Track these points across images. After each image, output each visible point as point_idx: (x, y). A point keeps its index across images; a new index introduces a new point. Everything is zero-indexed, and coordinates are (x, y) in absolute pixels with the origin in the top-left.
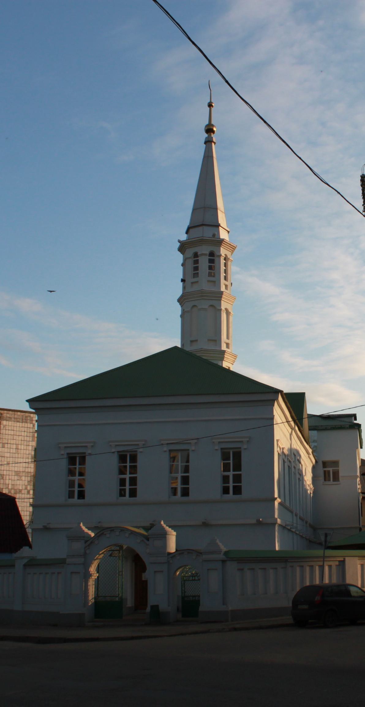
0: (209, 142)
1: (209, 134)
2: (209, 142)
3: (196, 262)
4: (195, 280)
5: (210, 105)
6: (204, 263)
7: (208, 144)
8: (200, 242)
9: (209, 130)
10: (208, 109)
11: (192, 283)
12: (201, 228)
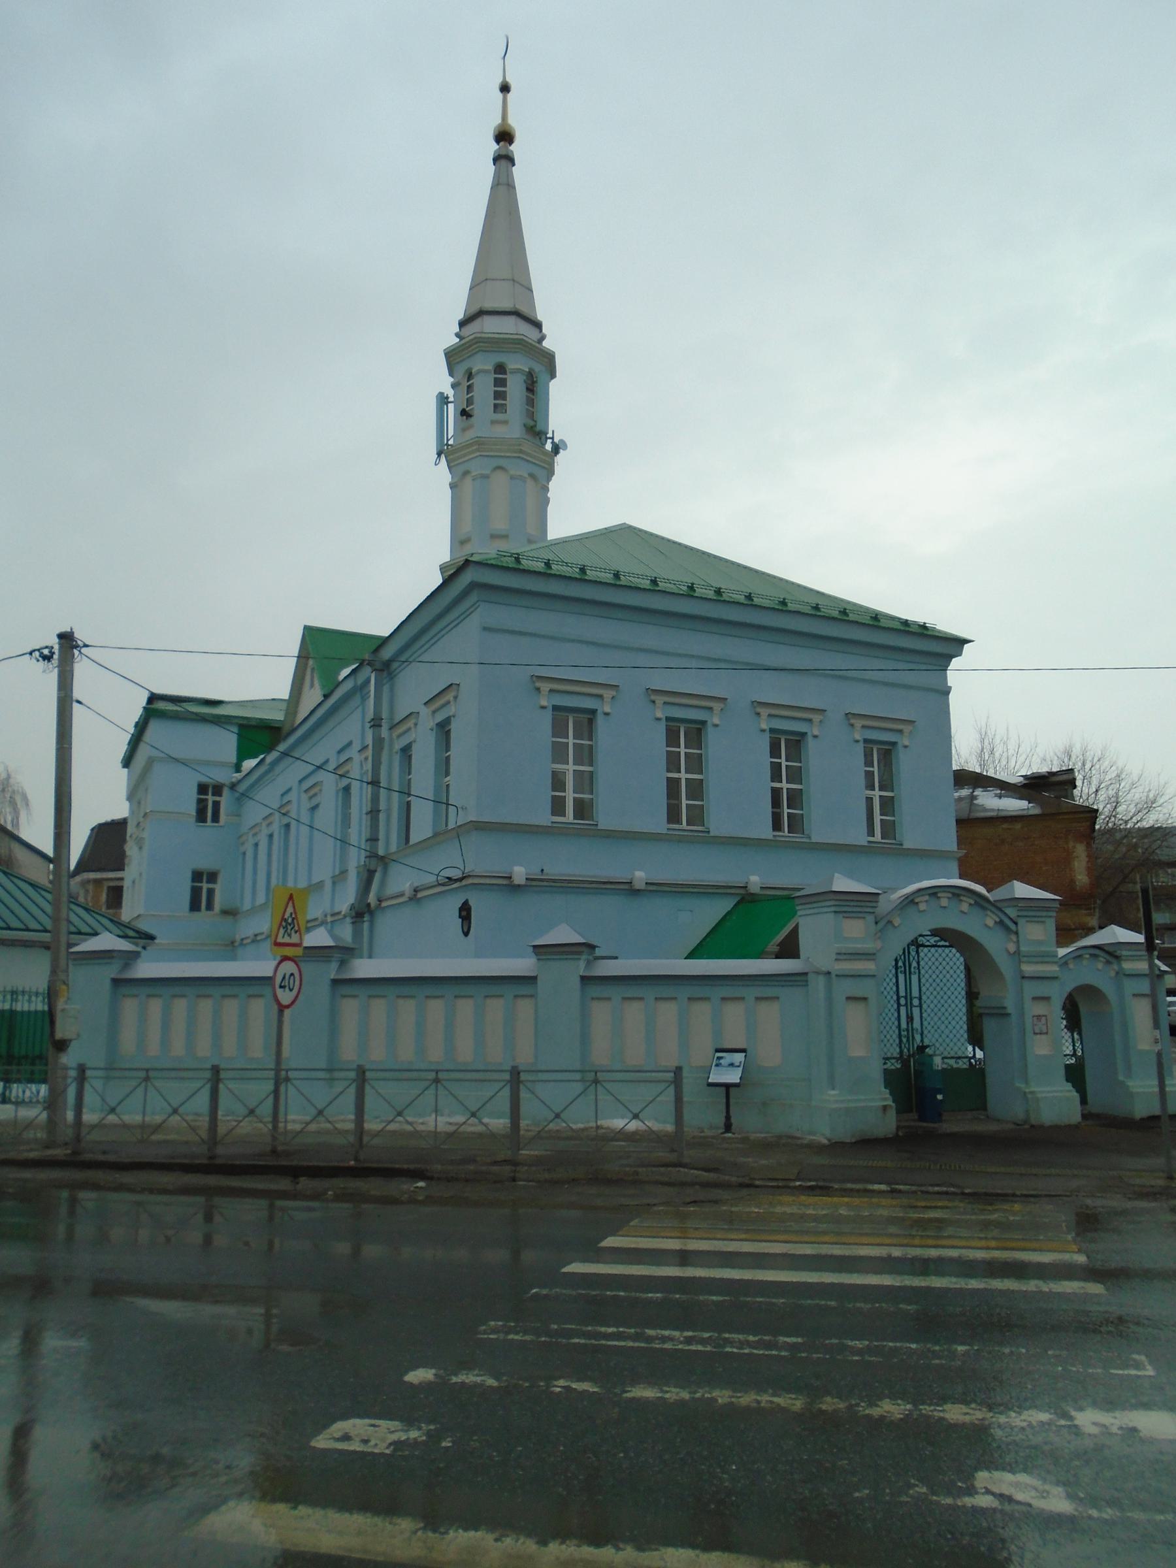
0: (504, 160)
1: (502, 143)
2: (504, 160)
4: (500, 416)
5: (505, 88)
6: (515, 388)
7: (503, 163)
9: (504, 136)
10: (500, 95)
11: (493, 422)
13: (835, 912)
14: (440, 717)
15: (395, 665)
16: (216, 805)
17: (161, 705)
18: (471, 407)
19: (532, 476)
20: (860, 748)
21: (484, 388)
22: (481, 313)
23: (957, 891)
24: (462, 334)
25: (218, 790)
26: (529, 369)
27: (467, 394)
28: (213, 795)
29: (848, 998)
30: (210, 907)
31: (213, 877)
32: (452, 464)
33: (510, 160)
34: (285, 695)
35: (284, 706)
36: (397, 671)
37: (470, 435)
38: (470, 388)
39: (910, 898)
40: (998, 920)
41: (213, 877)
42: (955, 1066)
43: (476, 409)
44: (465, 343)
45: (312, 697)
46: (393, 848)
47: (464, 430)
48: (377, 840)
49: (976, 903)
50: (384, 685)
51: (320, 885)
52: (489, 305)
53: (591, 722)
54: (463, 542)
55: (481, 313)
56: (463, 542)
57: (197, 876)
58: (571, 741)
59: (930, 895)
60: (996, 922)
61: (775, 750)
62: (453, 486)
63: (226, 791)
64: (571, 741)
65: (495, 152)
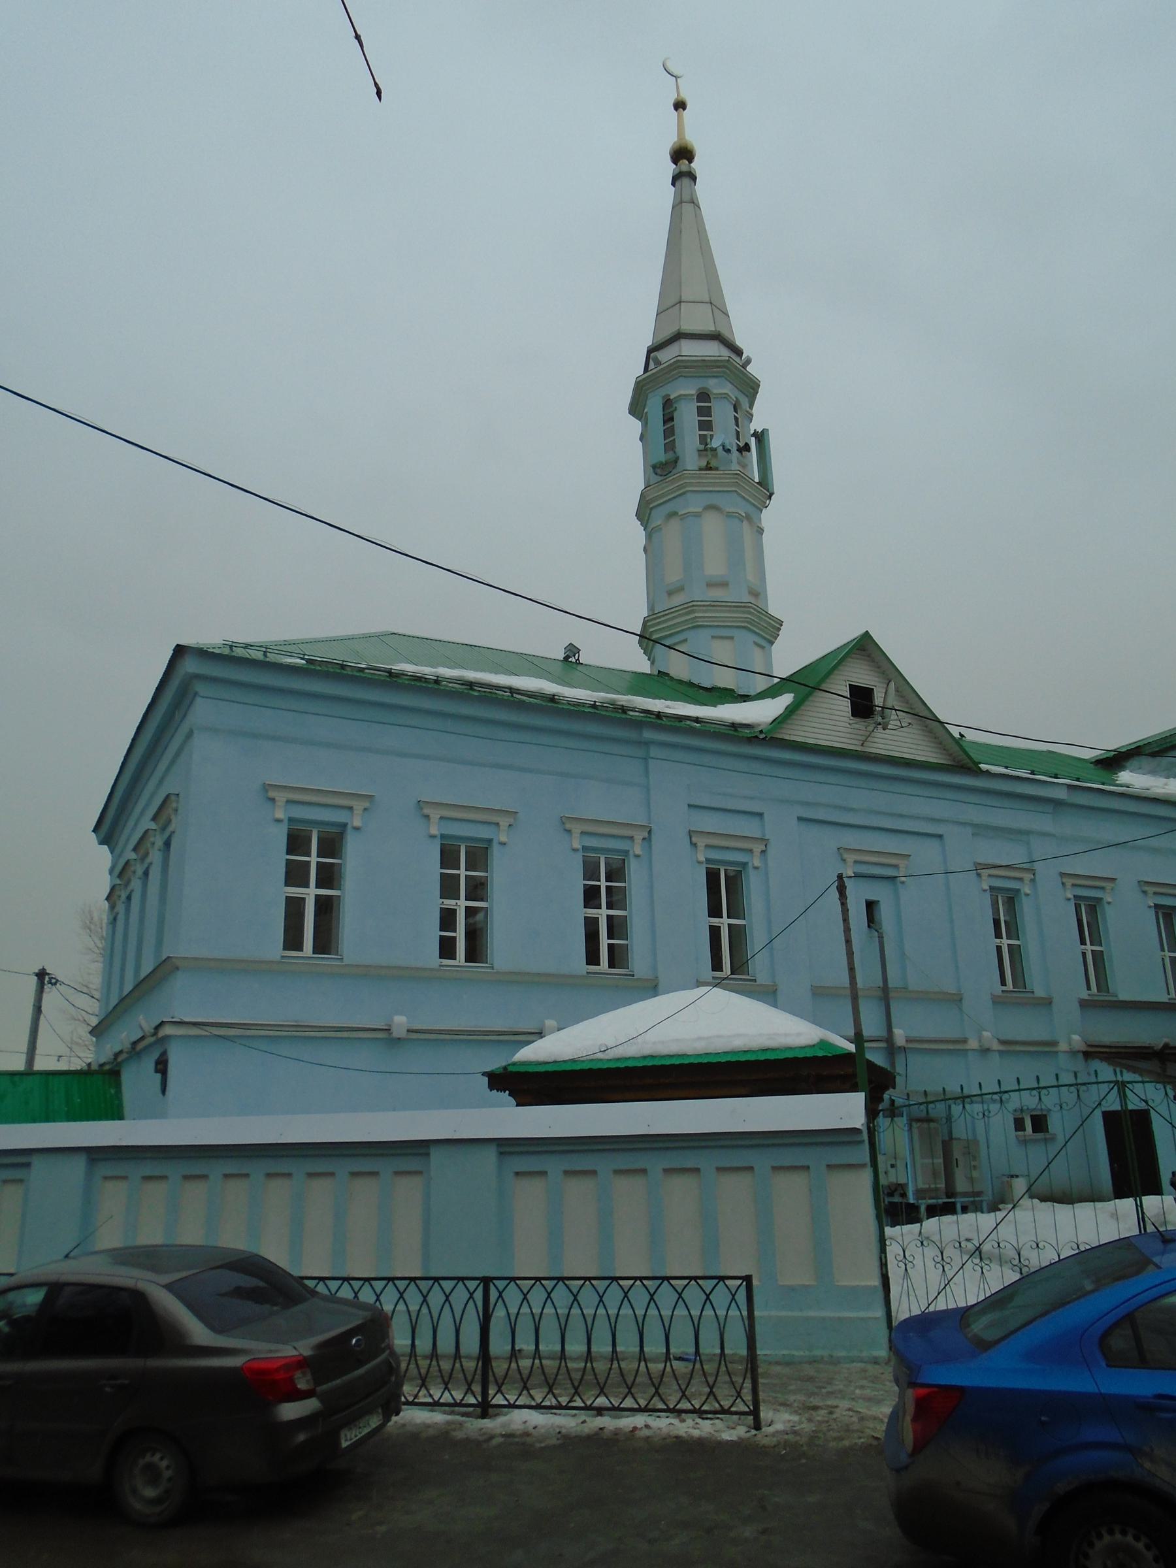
7: (686, 181)
9: (682, 154)
33: (693, 177)
52: (687, 327)
55: (679, 336)
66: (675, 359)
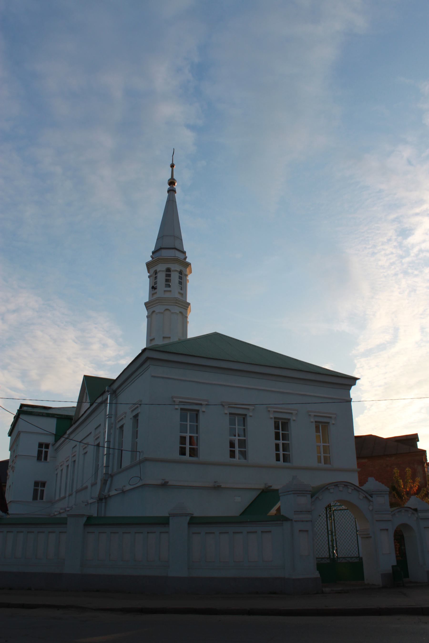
0: (172, 191)
1: (171, 185)
2: (172, 191)
3: (168, 276)
4: (168, 289)
5: (172, 166)
6: (175, 277)
7: (171, 192)
8: (174, 260)
9: (172, 182)
10: (171, 169)
11: (165, 291)
12: (174, 250)
13: (294, 494)
14: (135, 413)
15: (117, 392)
16: (46, 453)
17: (25, 409)
18: (156, 285)
19: (181, 312)
20: (314, 425)
21: (162, 277)
22: (161, 249)
23: (346, 484)
24: (153, 256)
25: (47, 446)
26: (180, 270)
27: (155, 280)
28: (45, 448)
29: (300, 531)
30: (42, 498)
31: (43, 484)
32: (148, 308)
33: (174, 191)
34: (75, 405)
35: (75, 409)
36: (118, 394)
37: (155, 296)
38: (156, 278)
39: (326, 487)
40: (364, 496)
41: (43, 484)
42: (351, 561)
43: (158, 285)
44: (155, 260)
45: (86, 406)
46: (115, 470)
47: (153, 294)
48: (109, 466)
49: (355, 489)
50: (113, 400)
51: (86, 488)
53: (197, 415)
54: (151, 340)
55: (161, 249)
56: (151, 340)
57: (36, 484)
58: (188, 423)
59: (335, 486)
60: (363, 497)
61: (277, 427)
62: (148, 317)
63: (50, 447)
64: (188, 423)
65: (168, 188)
66: (157, 258)
